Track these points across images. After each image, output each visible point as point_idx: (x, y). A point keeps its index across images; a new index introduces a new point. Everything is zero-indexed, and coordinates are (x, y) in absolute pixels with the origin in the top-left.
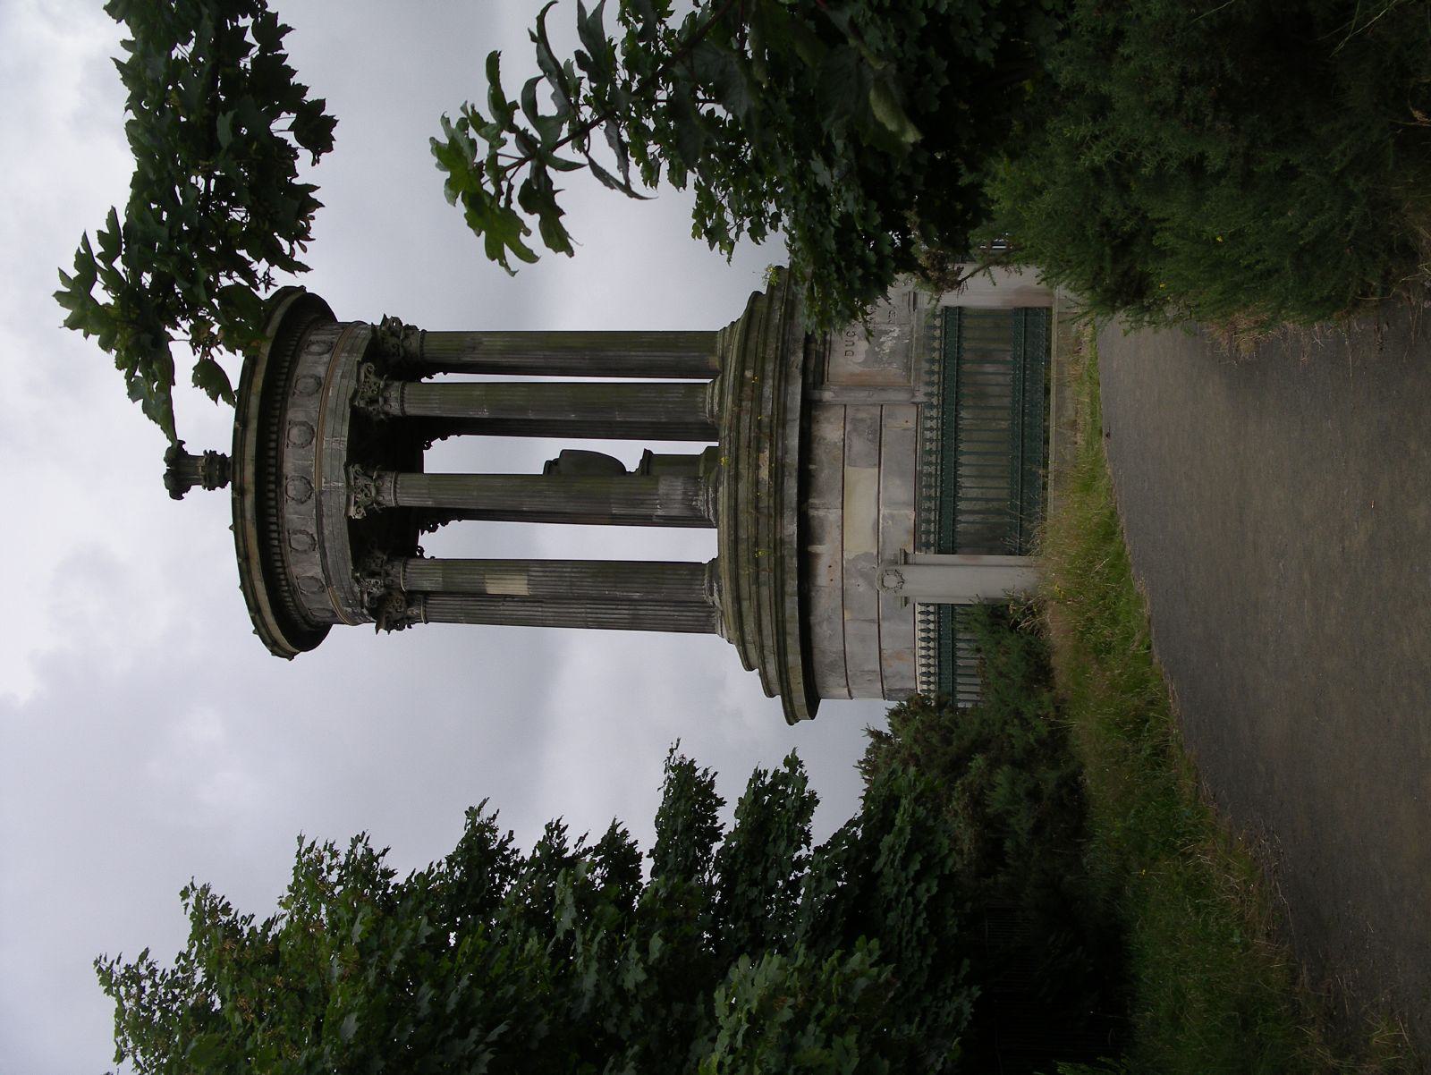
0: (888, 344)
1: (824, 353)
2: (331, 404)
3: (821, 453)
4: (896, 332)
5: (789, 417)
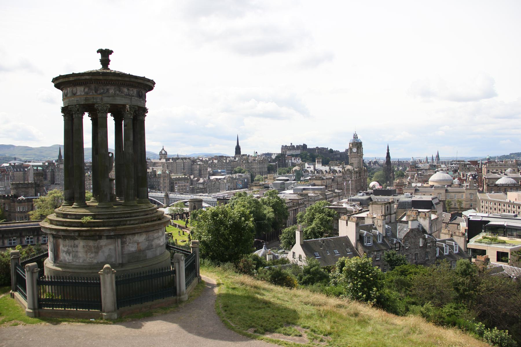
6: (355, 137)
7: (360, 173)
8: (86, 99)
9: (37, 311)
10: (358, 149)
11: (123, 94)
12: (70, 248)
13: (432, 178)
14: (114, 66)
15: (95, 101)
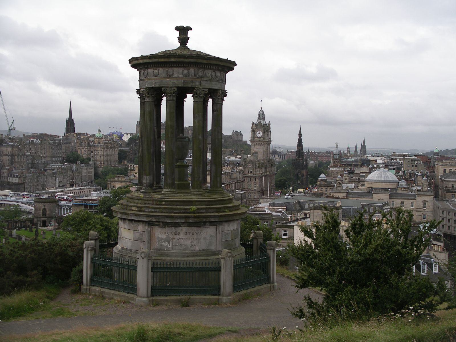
0: (165, 244)
1: (160, 226)
2: (164, 80)
3: (136, 224)
4: (170, 246)
5: (138, 217)
6: (261, 116)
7: (266, 168)
8: (184, 83)
9: (151, 299)
10: (264, 133)
11: (217, 79)
12: (170, 236)
13: (370, 177)
14: (191, 45)
15: (193, 84)
